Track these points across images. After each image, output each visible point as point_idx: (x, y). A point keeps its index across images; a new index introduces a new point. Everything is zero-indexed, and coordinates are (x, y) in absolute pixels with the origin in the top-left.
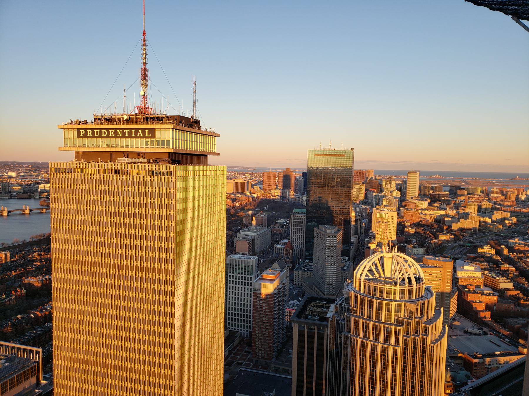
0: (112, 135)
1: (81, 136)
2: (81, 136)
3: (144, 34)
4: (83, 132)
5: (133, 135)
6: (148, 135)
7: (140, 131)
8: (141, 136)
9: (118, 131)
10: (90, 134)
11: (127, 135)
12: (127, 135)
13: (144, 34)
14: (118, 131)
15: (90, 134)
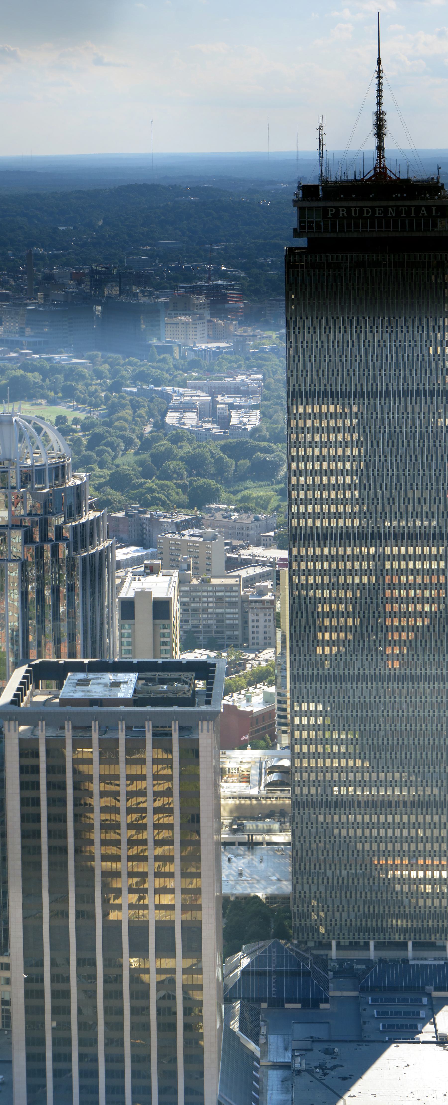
0: (379, 214)
1: (330, 216)
2: (330, 216)
3: (379, 63)
4: (332, 211)
5: (413, 215)
6: (436, 213)
7: (423, 208)
8: (426, 215)
9: (390, 209)
10: (343, 214)
11: (404, 215)
12: (404, 215)
13: (379, 63)
14: (390, 209)
15: (343, 214)
